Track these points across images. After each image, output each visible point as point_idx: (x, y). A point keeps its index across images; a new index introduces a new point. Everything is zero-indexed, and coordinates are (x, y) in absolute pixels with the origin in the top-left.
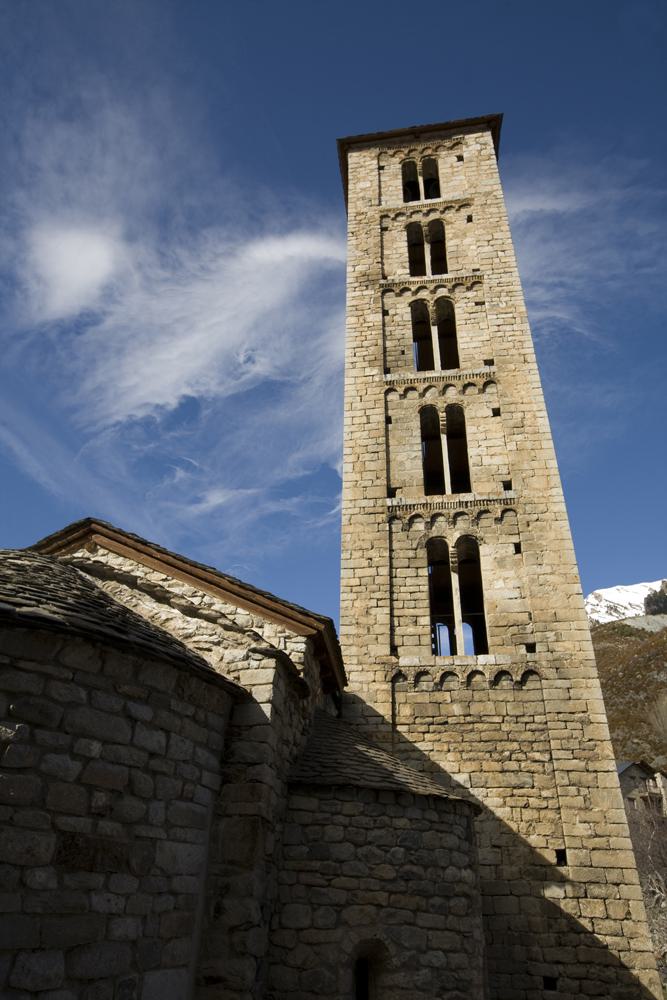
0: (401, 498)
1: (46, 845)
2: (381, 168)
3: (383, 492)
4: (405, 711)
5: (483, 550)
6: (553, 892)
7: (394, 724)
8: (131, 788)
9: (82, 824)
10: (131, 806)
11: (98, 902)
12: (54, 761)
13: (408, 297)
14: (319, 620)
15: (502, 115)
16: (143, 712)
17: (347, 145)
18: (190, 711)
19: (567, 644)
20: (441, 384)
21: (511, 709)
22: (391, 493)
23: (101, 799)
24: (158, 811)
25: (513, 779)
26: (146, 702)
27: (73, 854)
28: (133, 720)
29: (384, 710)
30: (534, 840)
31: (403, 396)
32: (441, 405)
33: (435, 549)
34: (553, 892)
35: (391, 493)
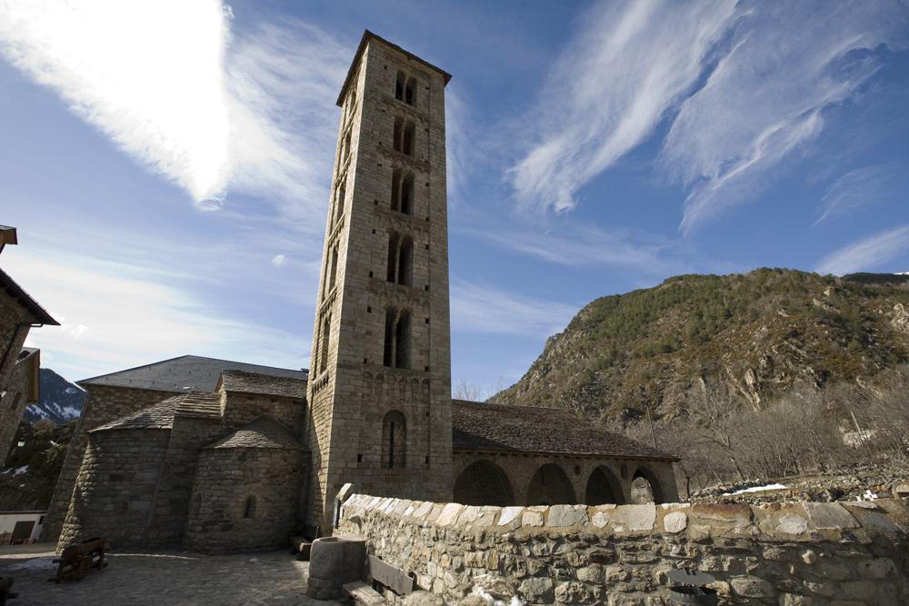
1: (106, 477)
7: (311, 410)
8: (127, 462)
9: (114, 472)
10: (127, 467)
11: (118, 488)
12: (109, 460)
14: (707, 277)
15: (366, 30)
16: (132, 444)
18: (150, 439)
23: (118, 466)
24: (136, 467)
26: (131, 441)
28: (128, 446)
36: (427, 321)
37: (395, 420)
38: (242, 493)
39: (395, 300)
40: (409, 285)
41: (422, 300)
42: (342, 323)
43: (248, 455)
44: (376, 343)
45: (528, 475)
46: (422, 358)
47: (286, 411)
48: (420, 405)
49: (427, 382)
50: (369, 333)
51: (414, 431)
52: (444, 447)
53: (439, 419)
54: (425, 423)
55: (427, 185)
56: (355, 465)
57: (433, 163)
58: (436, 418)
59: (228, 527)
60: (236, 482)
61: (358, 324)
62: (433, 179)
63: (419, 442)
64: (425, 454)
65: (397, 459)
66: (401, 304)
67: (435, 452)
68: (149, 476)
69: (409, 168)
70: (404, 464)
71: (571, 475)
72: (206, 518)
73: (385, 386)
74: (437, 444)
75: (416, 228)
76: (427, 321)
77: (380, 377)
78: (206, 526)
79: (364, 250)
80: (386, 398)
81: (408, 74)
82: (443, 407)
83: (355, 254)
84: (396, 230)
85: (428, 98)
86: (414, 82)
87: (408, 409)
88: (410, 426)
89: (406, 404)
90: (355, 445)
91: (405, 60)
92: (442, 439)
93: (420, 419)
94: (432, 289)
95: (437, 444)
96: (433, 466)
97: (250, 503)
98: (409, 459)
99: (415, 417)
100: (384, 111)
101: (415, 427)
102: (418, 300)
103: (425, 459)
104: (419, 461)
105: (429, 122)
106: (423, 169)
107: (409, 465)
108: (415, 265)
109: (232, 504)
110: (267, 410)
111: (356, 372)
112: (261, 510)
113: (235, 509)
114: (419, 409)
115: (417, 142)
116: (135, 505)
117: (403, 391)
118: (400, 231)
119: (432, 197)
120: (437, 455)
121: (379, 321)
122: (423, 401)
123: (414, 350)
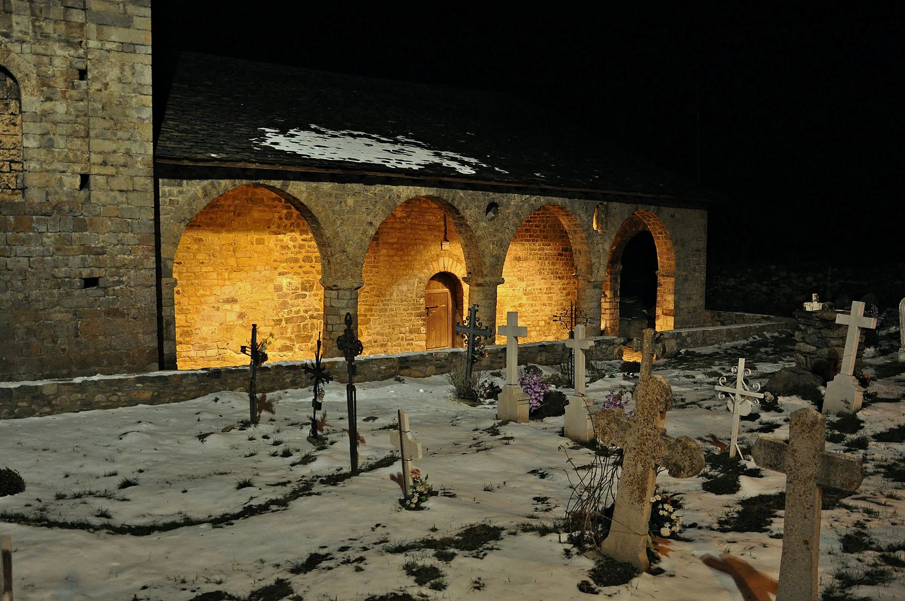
45: (369, 219)
48: (59, 52)
52: (128, 153)
53: (115, 88)
54: (74, 93)
58: (106, 85)
63: (61, 142)
64: (78, 168)
67: (104, 164)
71: (476, 221)
74: (108, 146)
82: (126, 56)
88: (31, 101)
89: (17, 48)
92: (120, 134)
93: (60, 84)
95: (108, 146)
96: (98, 195)
99: (44, 82)
101: (48, 105)
103: (77, 181)
104: (61, 183)
114: (57, 62)
120: (110, 170)
122: (68, 43)
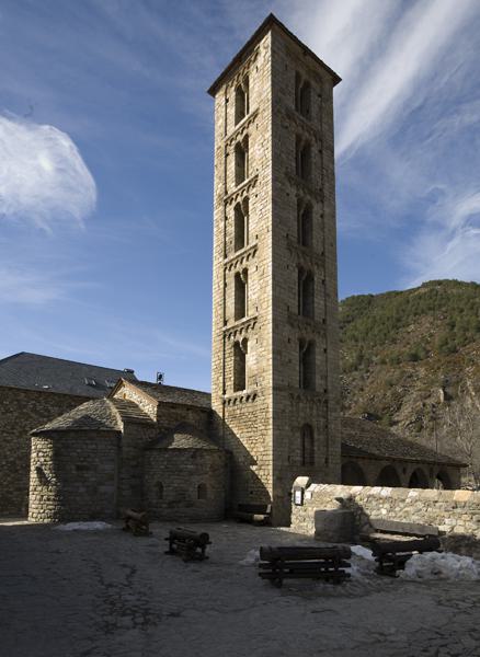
0: (229, 326)
1: (73, 467)
2: (227, 101)
3: (221, 324)
4: (227, 414)
5: (249, 344)
6: (254, 468)
8: (89, 456)
10: (89, 460)
13: (234, 203)
17: (213, 91)
19: (265, 382)
20: (240, 259)
21: (251, 410)
22: (225, 323)
25: (249, 434)
27: (79, 468)
29: (221, 415)
30: (252, 454)
31: (230, 270)
32: (241, 271)
33: (236, 344)
34: (254, 468)
35: (225, 323)
36: (325, 350)
37: (307, 430)
38: (196, 480)
39: (304, 331)
40: (313, 318)
41: (322, 332)
42: (273, 353)
43: (198, 454)
44: (295, 370)
46: (323, 382)
47: (198, 418)
49: (326, 402)
50: (290, 361)
51: (319, 440)
55: (322, 216)
56: (286, 464)
57: (326, 192)
59: (190, 505)
60: (191, 473)
61: (284, 354)
62: (327, 210)
65: (307, 460)
66: (309, 337)
68: (109, 467)
69: (308, 197)
70: (312, 463)
72: (171, 499)
73: (301, 405)
75: (317, 264)
76: (325, 350)
77: (299, 397)
78: (171, 505)
79: (283, 286)
80: (302, 414)
81: (304, 77)
83: (278, 288)
84: (302, 264)
85: (321, 108)
86: (307, 85)
87: (315, 424)
88: (316, 436)
90: (286, 449)
91: (301, 56)
94: (328, 322)
96: (330, 465)
97: (201, 488)
98: (316, 460)
100: (287, 127)
102: (319, 333)
105: (321, 141)
106: (319, 198)
107: (316, 465)
108: (316, 300)
109: (191, 489)
110: (184, 417)
111: (286, 394)
112: (211, 494)
113: (193, 492)
115: (313, 166)
116: (102, 489)
117: (311, 409)
118: (305, 266)
119: (326, 230)
121: (295, 351)
122: (324, 417)
123: (318, 376)
